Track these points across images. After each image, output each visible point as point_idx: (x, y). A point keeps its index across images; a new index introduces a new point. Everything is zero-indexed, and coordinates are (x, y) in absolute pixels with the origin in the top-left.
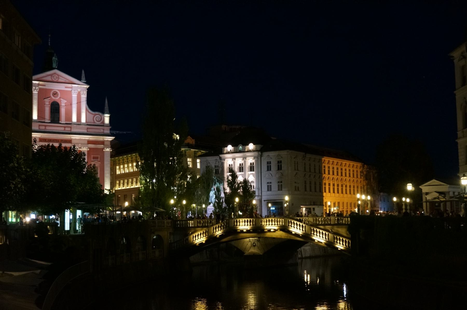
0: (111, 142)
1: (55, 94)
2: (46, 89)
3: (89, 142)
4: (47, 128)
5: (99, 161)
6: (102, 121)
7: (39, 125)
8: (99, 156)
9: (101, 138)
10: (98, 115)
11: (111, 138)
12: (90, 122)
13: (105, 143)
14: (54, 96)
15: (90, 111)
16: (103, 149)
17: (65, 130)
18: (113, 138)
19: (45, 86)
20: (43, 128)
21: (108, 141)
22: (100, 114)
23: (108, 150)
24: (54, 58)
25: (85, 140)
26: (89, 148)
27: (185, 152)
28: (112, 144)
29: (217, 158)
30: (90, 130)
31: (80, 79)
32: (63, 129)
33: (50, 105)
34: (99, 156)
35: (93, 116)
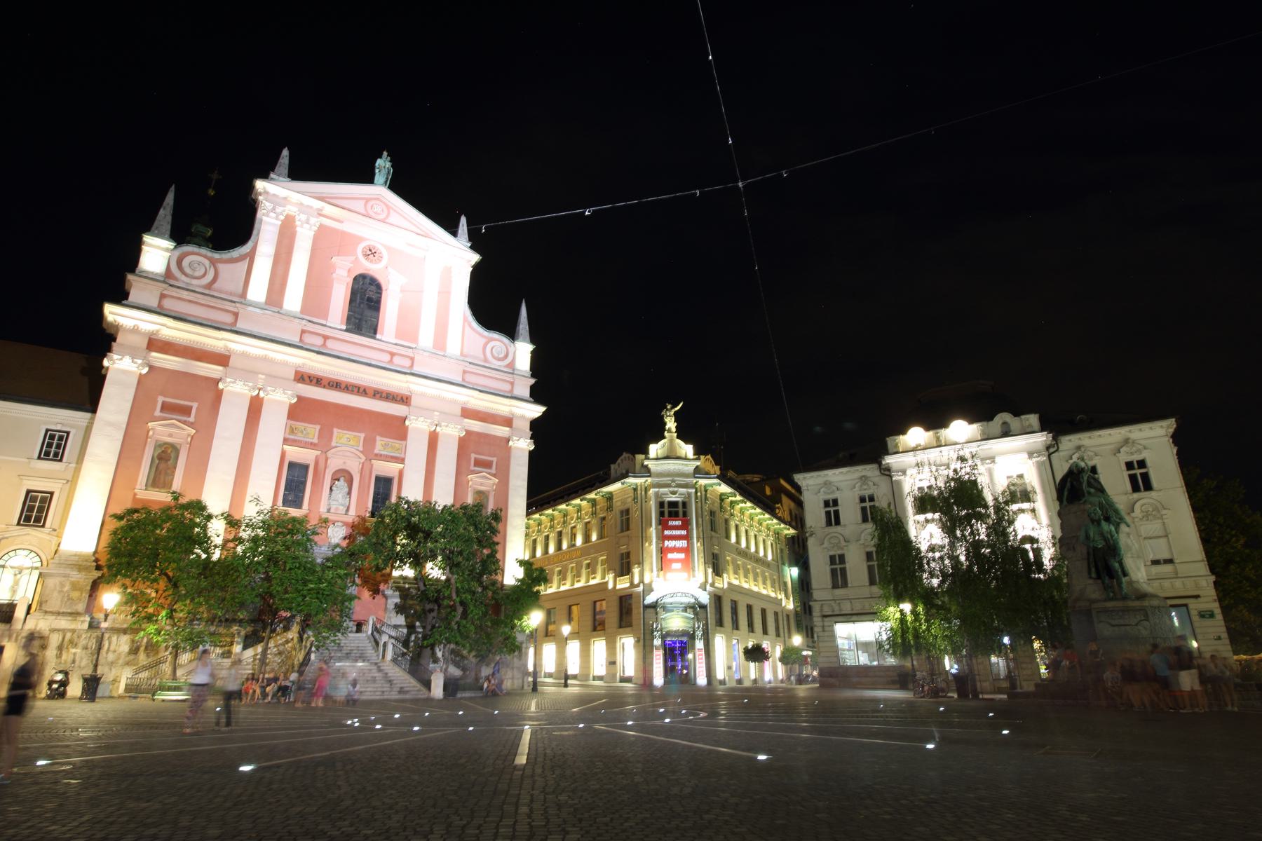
1: (371, 253)
2: (343, 233)
3: (467, 413)
4: (330, 343)
5: (494, 475)
7: (303, 332)
9: (503, 406)
10: (497, 340)
13: (515, 423)
14: (366, 256)
15: (475, 324)
17: (391, 361)
19: (340, 222)
20: (319, 341)
22: (505, 340)
23: (523, 445)
24: (379, 162)
25: (454, 402)
29: (869, 470)
30: (471, 379)
31: (452, 229)
32: (386, 357)
33: (350, 280)
34: (495, 460)
35: (484, 340)
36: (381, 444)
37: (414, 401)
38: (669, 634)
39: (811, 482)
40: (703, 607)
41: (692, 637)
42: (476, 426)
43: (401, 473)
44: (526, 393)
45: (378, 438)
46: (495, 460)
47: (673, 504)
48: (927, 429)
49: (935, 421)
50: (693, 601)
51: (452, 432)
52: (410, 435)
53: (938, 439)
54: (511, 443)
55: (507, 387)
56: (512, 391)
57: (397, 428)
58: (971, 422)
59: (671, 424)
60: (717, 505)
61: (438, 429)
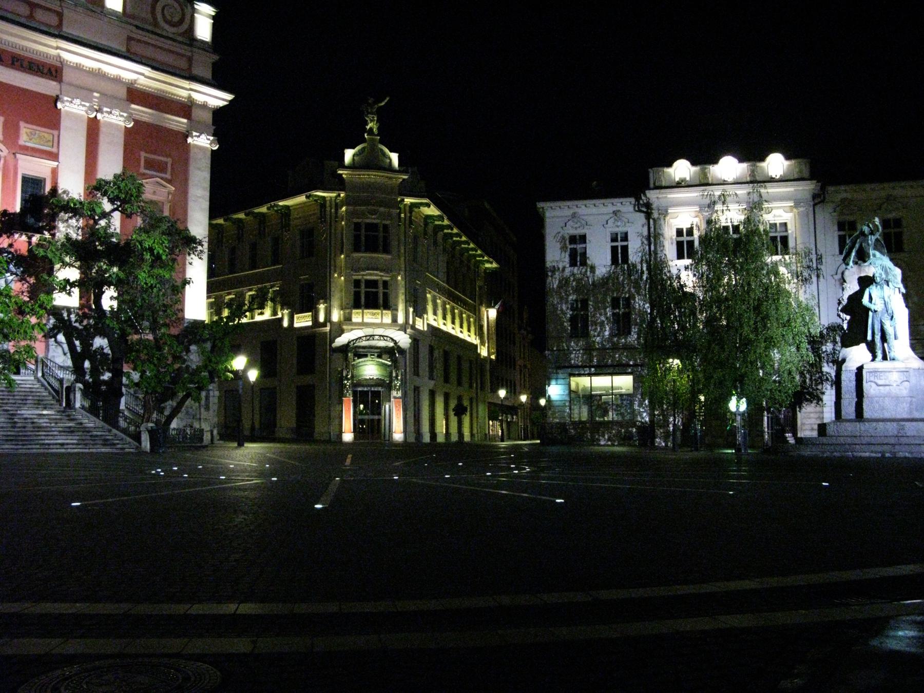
0: (218, 113)
3: (135, 95)
6: (185, 26)
8: (169, 160)
11: (217, 98)
12: (143, 20)
13: (196, 113)
16: (186, 136)
18: (229, 97)
21: (204, 106)
23: (203, 142)
25: (117, 80)
26: (137, 122)
27: (411, 212)
28: (221, 121)
29: (626, 205)
36: (27, 134)
37: (67, 75)
38: (359, 384)
39: (558, 213)
40: (402, 351)
41: (389, 387)
42: (144, 113)
43: (55, 172)
44: (208, 75)
45: (22, 124)
46: (169, 160)
47: (372, 227)
48: (694, 163)
49: (704, 156)
50: (391, 344)
51: (116, 120)
52: (64, 123)
53: (704, 174)
54: (190, 140)
55: (183, 64)
56: (190, 68)
57: (46, 113)
58: (741, 160)
59: (372, 125)
60: (421, 229)
61: (99, 116)
